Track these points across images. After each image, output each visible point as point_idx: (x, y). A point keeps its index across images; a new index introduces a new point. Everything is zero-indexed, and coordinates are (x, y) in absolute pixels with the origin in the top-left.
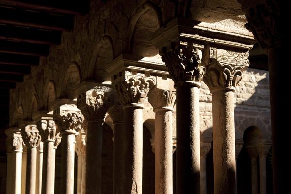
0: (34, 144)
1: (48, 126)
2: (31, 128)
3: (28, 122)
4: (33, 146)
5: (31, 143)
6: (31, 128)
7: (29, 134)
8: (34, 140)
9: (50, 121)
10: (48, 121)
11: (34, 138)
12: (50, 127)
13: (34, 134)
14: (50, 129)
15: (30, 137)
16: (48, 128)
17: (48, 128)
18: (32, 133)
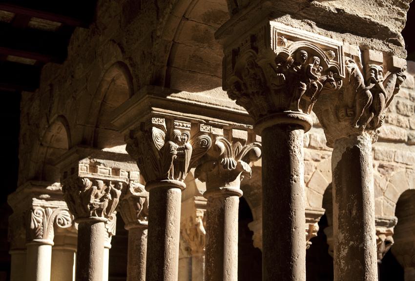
0: (99, 212)
1: (170, 136)
2: (93, 168)
3: (88, 150)
4: (97, 217)
5: (92, 208)
6: (93, 168)
7: (89, 183)
8: (102, 200)
9: (176, 123)
10: (170, 120)
11: (101, 195)
12: (176, 140)
13: (102, 184)
14: (174, 146)
15: (91, 190)
16: (172, 143)
17: (172, 143)
18: (95, 182)
